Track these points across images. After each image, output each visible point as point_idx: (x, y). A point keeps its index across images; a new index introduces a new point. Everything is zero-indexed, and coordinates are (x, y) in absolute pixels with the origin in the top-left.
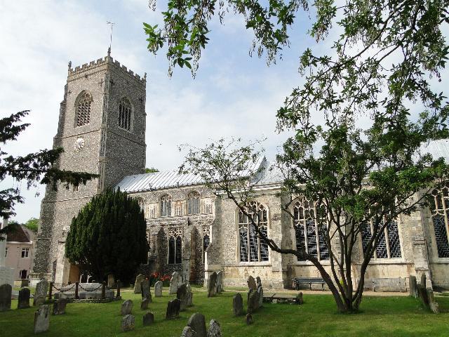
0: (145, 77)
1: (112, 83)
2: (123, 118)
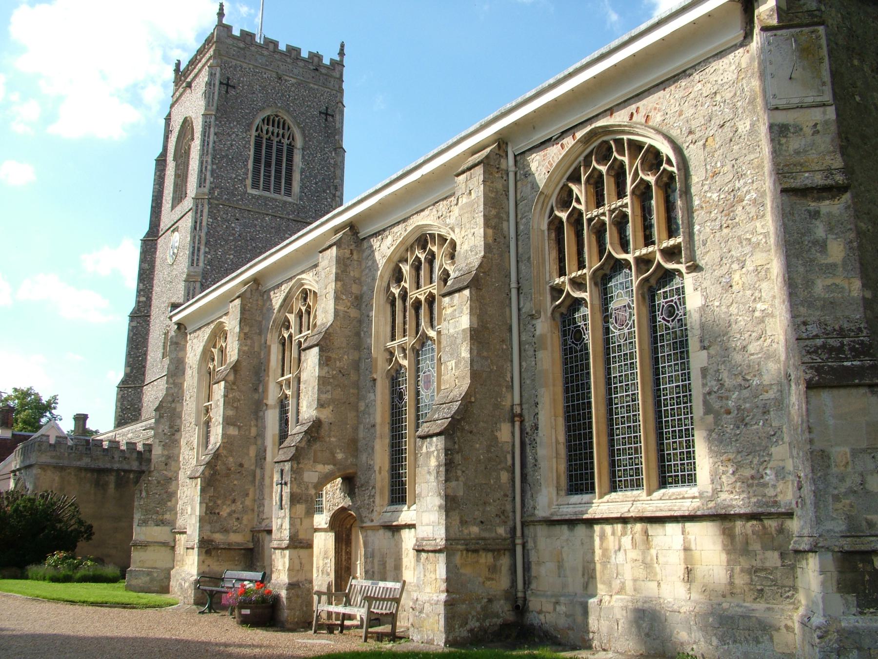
0: (342, 53)
1: (227, 84)
2: (268, 165)
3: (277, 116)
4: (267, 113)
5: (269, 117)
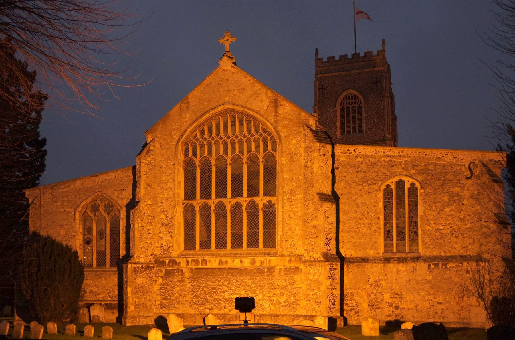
3: (350, 94)
4: (344, 94)
5: (346, 95)
